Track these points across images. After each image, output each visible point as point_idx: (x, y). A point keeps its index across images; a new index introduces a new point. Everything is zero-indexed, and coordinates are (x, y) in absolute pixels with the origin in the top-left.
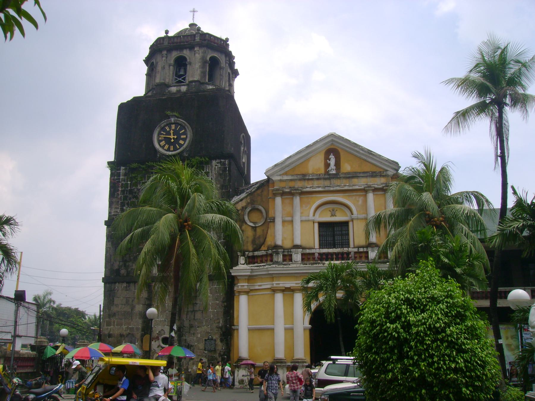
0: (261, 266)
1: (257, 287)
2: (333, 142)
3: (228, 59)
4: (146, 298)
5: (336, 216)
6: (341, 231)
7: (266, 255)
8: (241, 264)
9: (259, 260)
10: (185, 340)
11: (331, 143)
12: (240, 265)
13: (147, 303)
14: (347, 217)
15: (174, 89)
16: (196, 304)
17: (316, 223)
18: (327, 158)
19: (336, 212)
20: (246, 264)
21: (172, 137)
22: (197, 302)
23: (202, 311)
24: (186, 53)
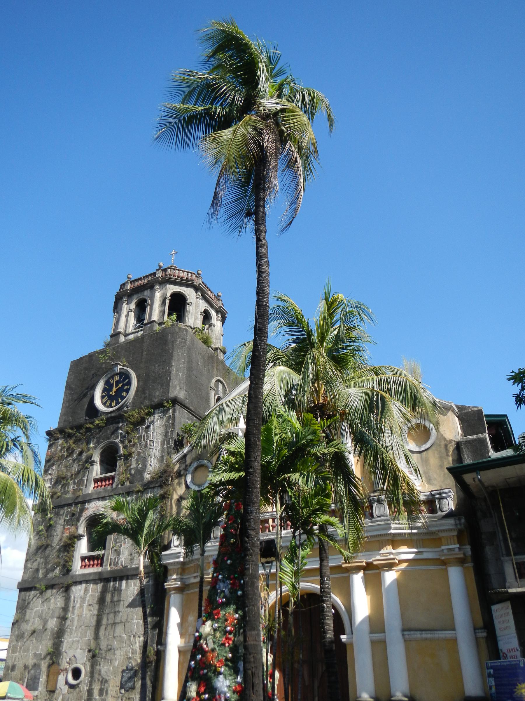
3: (199, 293)
4: (62, 608)
10: (100, 671)
12: (173, 548)
13: (62, 614)
15: (131, 337)
16: (118, 613)
21: (114, 390)
22: (120, 610)
23: (124, 624)
24: (147, 293)
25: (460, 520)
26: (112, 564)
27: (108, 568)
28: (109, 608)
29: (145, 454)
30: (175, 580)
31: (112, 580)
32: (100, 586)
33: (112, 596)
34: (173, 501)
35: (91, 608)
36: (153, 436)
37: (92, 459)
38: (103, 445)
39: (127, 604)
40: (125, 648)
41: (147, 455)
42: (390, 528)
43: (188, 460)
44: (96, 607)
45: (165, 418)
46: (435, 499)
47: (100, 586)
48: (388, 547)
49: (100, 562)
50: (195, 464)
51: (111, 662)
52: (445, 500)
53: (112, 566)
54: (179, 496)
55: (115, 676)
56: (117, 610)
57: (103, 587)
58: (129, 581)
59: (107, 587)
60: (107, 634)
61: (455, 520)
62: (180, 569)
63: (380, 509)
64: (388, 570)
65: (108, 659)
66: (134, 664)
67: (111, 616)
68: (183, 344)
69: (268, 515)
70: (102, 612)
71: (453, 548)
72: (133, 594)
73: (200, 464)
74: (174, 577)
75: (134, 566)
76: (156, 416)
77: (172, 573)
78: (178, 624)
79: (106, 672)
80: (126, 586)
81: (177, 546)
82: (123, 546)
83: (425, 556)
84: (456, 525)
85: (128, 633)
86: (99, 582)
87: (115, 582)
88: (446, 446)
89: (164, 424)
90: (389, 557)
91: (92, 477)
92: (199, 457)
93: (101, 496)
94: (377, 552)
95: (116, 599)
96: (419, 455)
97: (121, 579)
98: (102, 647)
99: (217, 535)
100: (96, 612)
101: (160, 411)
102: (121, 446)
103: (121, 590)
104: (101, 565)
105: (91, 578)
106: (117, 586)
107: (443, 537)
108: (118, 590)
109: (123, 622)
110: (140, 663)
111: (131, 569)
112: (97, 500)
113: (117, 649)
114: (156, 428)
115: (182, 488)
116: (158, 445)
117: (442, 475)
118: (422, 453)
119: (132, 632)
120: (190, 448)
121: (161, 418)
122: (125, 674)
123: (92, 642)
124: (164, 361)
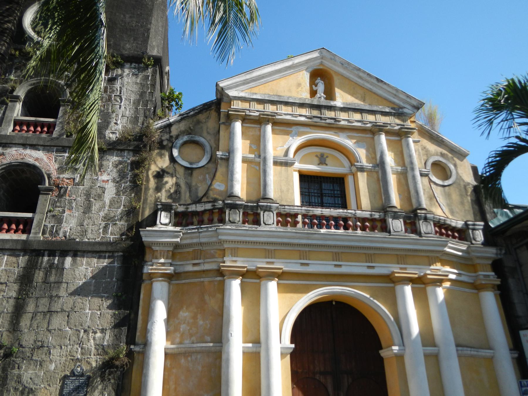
0: (201, 228)
1: (190, 268)
2: (323, 61)
5: (327, 165)
6: (334, 190)
7: (211, 211)
8: (161, 224)
9: (195, 220)
10: (19, 377)
11: (319, 61)
14: (343, 169)
16: (56, 299)
17: (295, 171)
18: (313, 82)
19: (327, 159)
20: (170, 224)
22: (60, 294)
23: (67, 313)
25: (501, 250)
26: (48, 233)
27: (40, 237)
28: (40, 290)
29: (108, 109)
30: (163, 264)
31: (46, 253)
32: (22, 260)
33: (46, 274)
34: (150, 173)
35: (4, 288)
36: (121, 91)
37: (15, 94)
38: (35, 82)
39: (72, 288)
40: (69, 347)
41: (110, 111)
42: (445, 246)
43: (174, 131)
44: (16, 287)
45: (140, 76)
46: (468, 229)
47: (22, 260)
48: (437, 264)
49: (21, 227)
50: (185, 138)
51: (41, 365)
52: (477, 232)
53: (47, 235)
54: (159, 168)
55: (49, 385)
56: (54, 293)
57: (29, 261)
58: (78, 258)
59: (37, 262)
60: (35, 325)
61: (497, 250)
62: (171, 253)
63: (427, 226)
64: (440, 286)
65: (36, 361)
66: (85, 367)
67: (44, 301)
68: (162, 7)
69: (301, 210)
70: (27, 294)
71: (489, 275)
72: (85, 275)
73: (192, 139)
74: (162, 260)
75: (87, 240)
76: (127, 71)
77: (159, 255)
78: (164, 320)
79: (31, 379)
80: (72, 265)
81: (166, 225)
82: (67, 213)
83: (463, 278)
84: (497, 254)
85: (75, 326)
86: (22, 254)
87: (52, 258)
88: (465, 187)
89: (138, 82)
90: (440, 273)
91: (12, 117)
92: (190, 131)
93: (31, 143)
94: (427, 267)
95: (52, 279)
96: (442, 188)
97: (64, 254)
98: (24, 343)
99: (235, 220)
100: (14, 294)
101: (133, 66)
102: (68, 91)
103: (63, 269)
104: (27, 230)
105: (7, 246)
106: (56, 262)
107: (479, 264)
108: (57, 268)
109: (65, 311)
110: (96, 367)
111: (79, 242)
112: (21, 146)
113: (54, 347)
114: (125, 83)
115: (164, 160)
116: (128, 103)
117: (463, 210)
118: (445, 188)
119: (82, 325)
120: (180, 118)
121: (132, 74)
122: (68, 382)
123: (4, 335)
124: (138, 14)
